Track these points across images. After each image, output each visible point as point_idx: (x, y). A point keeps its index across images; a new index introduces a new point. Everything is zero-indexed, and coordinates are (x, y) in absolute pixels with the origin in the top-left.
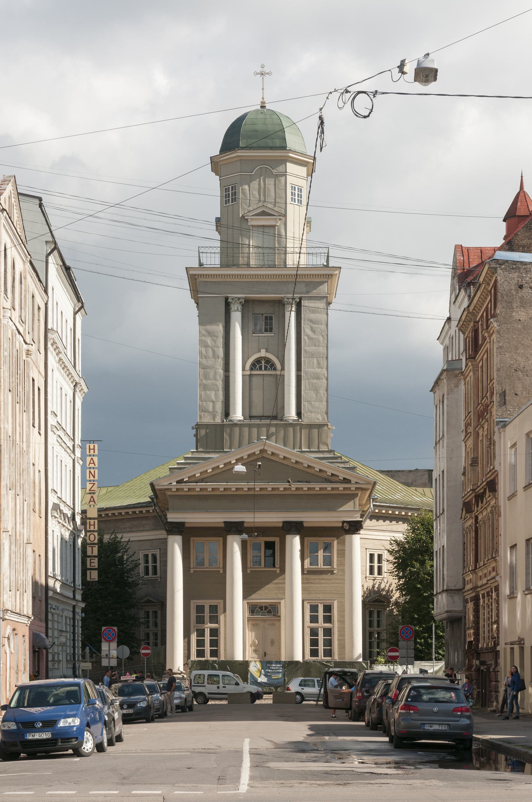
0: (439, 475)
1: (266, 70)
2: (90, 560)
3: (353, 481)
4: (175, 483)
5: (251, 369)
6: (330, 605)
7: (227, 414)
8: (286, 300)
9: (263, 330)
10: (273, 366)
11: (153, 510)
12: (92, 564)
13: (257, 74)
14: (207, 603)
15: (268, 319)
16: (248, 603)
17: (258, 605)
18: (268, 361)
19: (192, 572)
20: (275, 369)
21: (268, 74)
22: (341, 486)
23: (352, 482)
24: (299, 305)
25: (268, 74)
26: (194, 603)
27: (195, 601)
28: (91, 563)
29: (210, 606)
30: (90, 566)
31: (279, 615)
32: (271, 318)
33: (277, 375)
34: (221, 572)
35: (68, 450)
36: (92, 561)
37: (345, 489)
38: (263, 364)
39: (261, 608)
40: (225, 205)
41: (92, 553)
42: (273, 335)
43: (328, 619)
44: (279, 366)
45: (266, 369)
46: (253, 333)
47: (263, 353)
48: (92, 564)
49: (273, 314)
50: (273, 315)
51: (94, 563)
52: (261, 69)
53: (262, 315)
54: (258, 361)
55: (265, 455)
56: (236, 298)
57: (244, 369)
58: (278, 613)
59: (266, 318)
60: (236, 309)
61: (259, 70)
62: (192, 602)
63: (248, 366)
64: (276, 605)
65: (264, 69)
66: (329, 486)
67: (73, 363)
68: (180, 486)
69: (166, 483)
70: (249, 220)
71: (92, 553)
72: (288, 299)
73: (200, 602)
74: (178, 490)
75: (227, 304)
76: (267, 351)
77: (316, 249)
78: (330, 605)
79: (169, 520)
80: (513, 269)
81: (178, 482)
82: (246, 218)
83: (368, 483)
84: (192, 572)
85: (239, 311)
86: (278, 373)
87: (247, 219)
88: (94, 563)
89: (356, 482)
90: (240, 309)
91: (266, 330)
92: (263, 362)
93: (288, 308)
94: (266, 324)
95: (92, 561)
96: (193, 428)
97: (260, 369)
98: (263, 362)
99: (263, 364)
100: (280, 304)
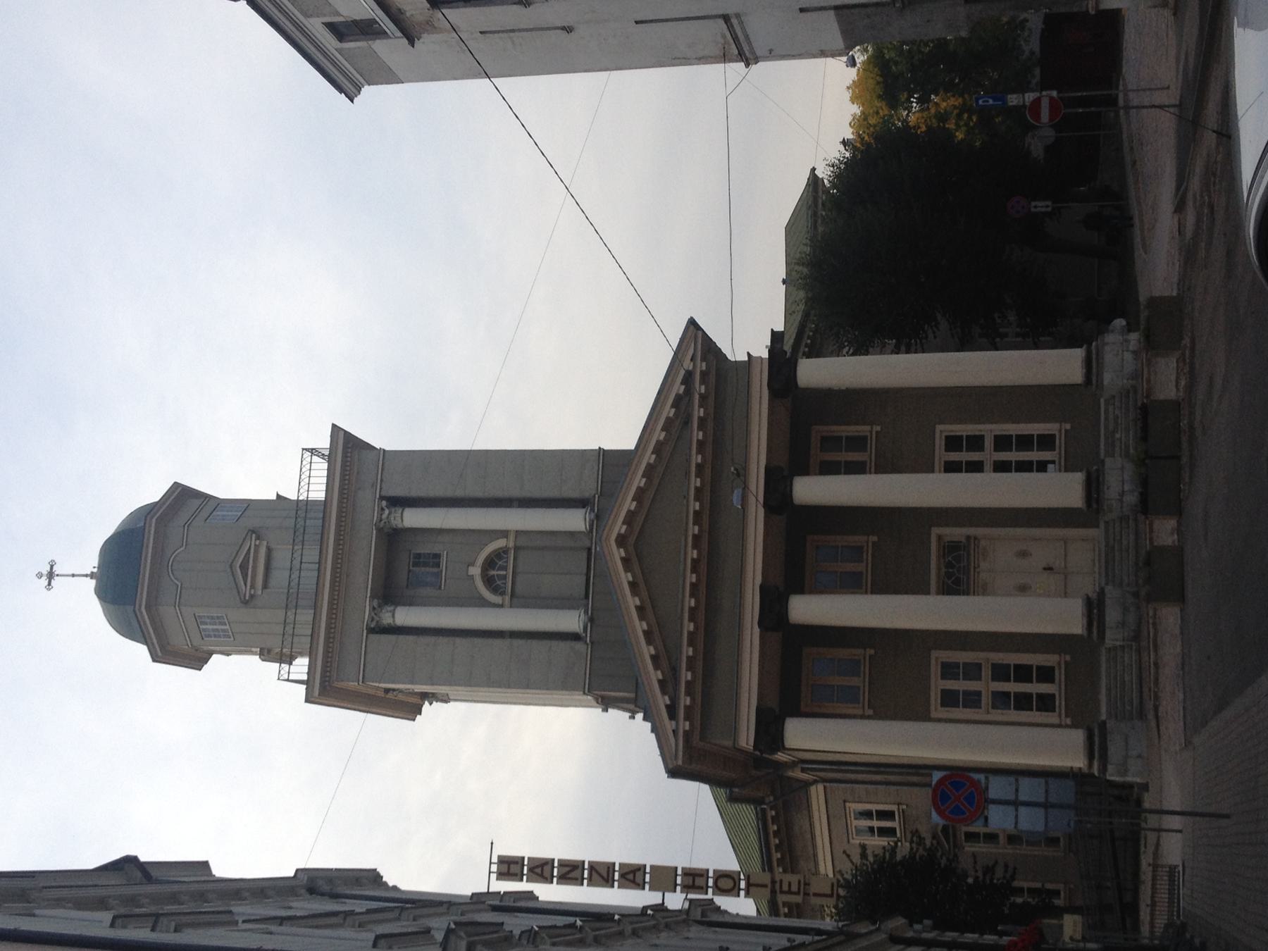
1: (47, 568)
2: (782, 892)
3: (688, 365)
5: (503, 594)
6: (947, 437)
7: (575, 637)
9: (435, 570)
10: (500, 554)
11: (771, 809)
12: (794, 888)
13: (49, 584)
15: (419, 560)
17: (943, 582)
18: (490, 563)
21: (52, 567)
23: (691, 368)
25: (52, 567)
26: (937, 711)
27: (933, 708)
28: (790, 892)
29: (944, 677)
30: (798, 893)
31: (963, 540)
32: (419, 556)
33: (517, 549)
36: (785, 888)
37: (703, 381)
40: (232, 639)
41: (765, 886)
42: (445, 553)
43: (976, 443)
44: (500, 543)
45: (505, 568)
46: (440, 588)
47: (476, 571)
48: (794, 888)
49: (410, 551)
50: (412, 552)
51: (790, 884)
52: (44, 578)
53: (409, 571)
54: (489, 582)
55: (632, 540)
56: (370, 614)
58: (961, 542)
59: (415, 564)
60: (390, 614)
61: (44, 581)
62: (934, 715)
63: (496, 599)
64: (944, 547)
65: (45, 572)
68: (681, 713)
69: (672, 740)
70: (252, 592)
71: (765, 886)
72: (381, 521)
73: (935, 698)
76: (472, 564)
77: (303, 470)
78: (947, 437)
82: (247, 598)
85: (394, 610)
87: (252, 596)
88: (790, 884)
89: (691, 360)
91: (438, 565)
93: (396, 522)
94: (426, 565)
95: (785, 888)
97: (505, 577)
100: (392, 538)
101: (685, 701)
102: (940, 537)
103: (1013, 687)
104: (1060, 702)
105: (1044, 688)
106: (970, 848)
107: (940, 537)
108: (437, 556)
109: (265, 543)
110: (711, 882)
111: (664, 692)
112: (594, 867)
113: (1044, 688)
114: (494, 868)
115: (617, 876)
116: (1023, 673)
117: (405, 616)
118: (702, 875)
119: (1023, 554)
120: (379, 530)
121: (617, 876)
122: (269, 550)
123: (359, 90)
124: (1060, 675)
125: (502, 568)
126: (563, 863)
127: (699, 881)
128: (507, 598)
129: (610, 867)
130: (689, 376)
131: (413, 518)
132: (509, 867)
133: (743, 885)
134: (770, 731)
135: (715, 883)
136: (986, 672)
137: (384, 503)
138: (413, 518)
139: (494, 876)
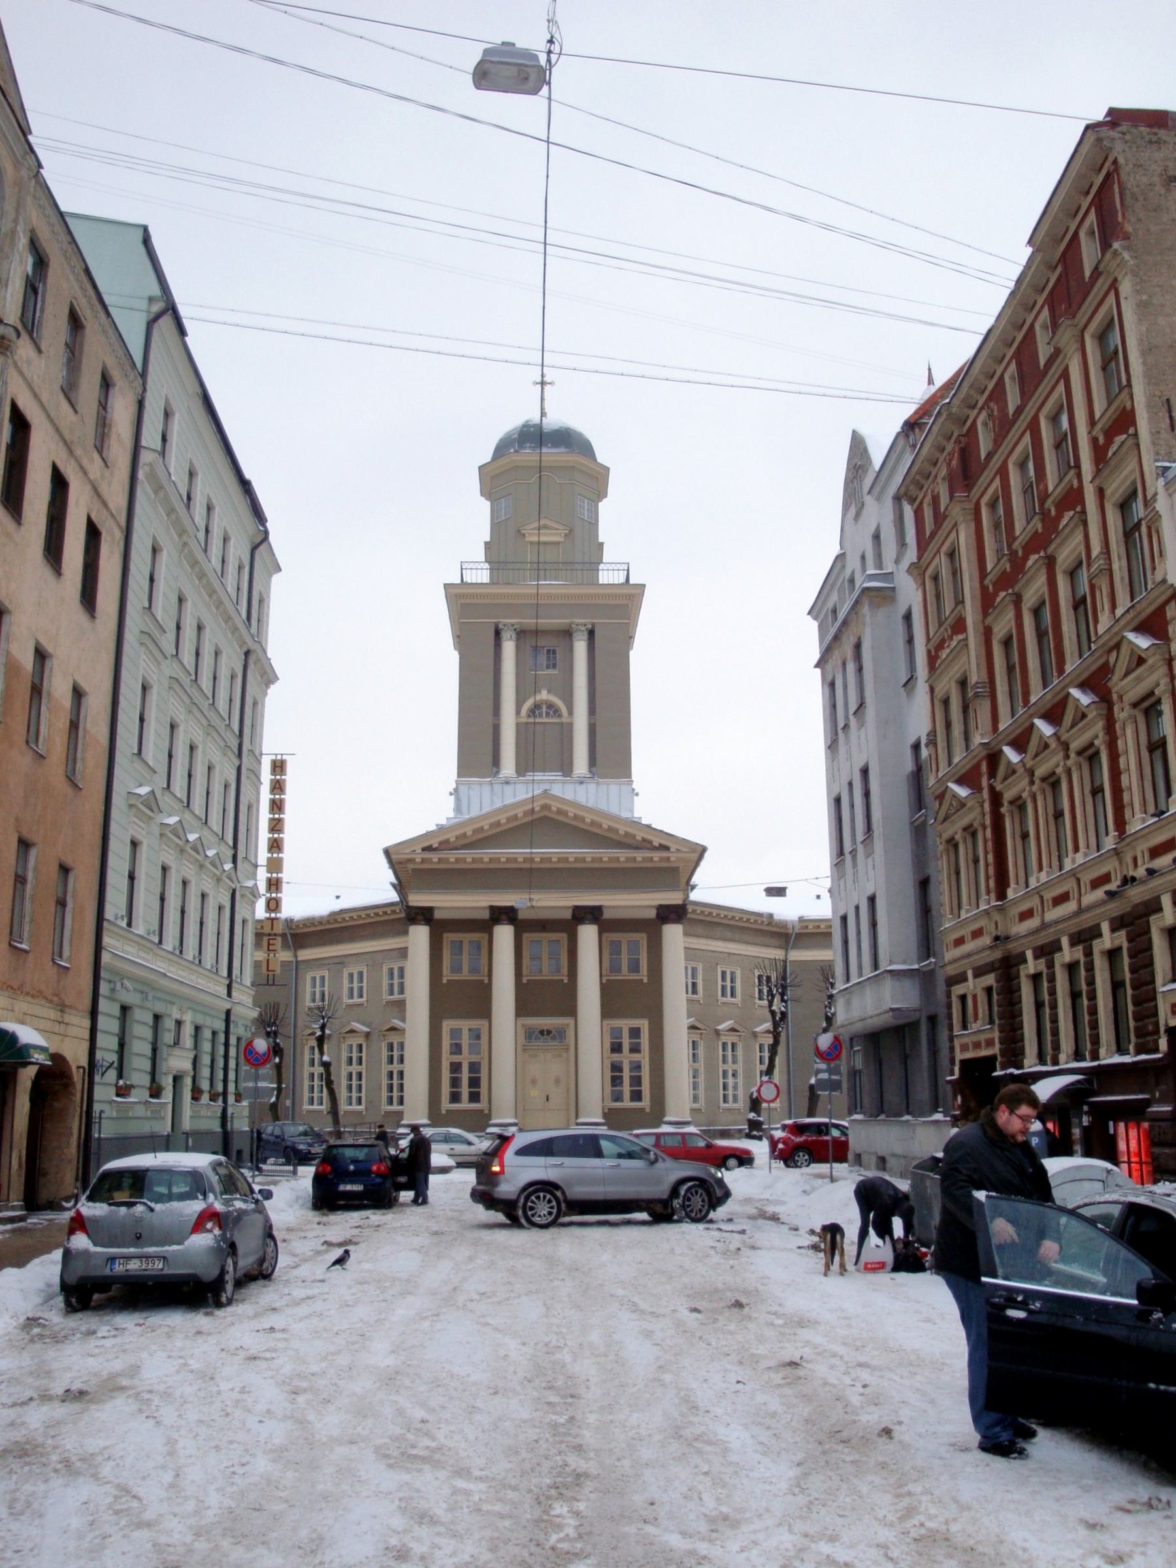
0: (850, 784)
4: (420, 851)
5: (529, 716)
8: (573, 626)
10: (557, 712)
14: (465, 1025)
15: (551, 652)
16: (523, 1025)
18: (550, 706)
19: (445, 981)
20: (560, 716)
21: (550, 383)
22: (657, 856)
23: (672, 850)
24: (591, 633)
25: (550, 383)
28: (269, 944)
32: (554, 652)
33: (562, 724)
34: (486, 981)
35: (230, 754)
36: (271, 942)
37: (661, 859)
38: (544, 710)
39: (542, 1032)
43: (635, 1049)
45: (548, 714)
47: (544, 695)
54: (537, 707)
57: (518, 712)
59: (549, 651)
66: (640, 855)
67: (203, 545)
68: (427, 855)
69: (408, 851)
74: (423, 860)
75: (497, 633)
76: (549, 692)
79: (411, 904)
80: (1150, 142)
81: (423, 849)
83: (694, 851)
84: (445, 981)
86: (565, 719)
90: (514, 638)
91: (548, 667)
92: (544, 707)
93: (576, 636)
94: (548, 658)
96: (451, 794)
98: (544, 707)
99: (544, 710)
100: (567, 634)
101: (435, 857)
102: (568, 1025)
103: (465, 1076)
104: (455, 1106)
105: (465, 1095)
106: (384, 1046)
107: (568, 1025)
108: (554, 666)
109: (562, 540)
110: (274, 895)
111: (440, 843)
112: (280, 820)
113: (465, 1095)
114: (279, 757)
115: (276, 836)
116: (455, 1082)
117: (509, 648)
118: (277, 889)
119: (557, 1081)
120: (570, 624)
121: (276, 836)
122: (558, 543)
123: (815, 618)
124: (474, 1106)
125: (548, 714)
126: (282, 801)
127: (273, 888)
128: (524, 720)
129: (280, 831)
130: (667, 848)
131: (580, 648)
132: (279, 766)
133: (273, 915)
134: (423, 915)
135: (274, 899)
136: (474, 1058)
137: (590, 626)
138: (580, 648)
139: (274, 757)
